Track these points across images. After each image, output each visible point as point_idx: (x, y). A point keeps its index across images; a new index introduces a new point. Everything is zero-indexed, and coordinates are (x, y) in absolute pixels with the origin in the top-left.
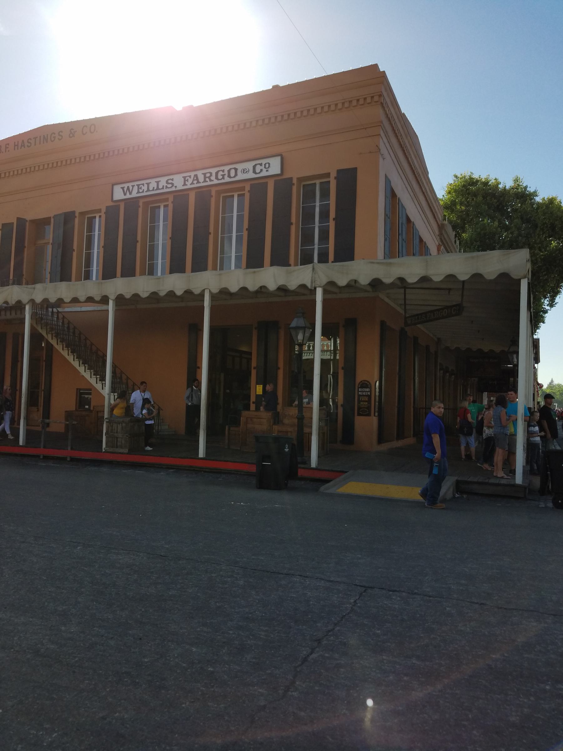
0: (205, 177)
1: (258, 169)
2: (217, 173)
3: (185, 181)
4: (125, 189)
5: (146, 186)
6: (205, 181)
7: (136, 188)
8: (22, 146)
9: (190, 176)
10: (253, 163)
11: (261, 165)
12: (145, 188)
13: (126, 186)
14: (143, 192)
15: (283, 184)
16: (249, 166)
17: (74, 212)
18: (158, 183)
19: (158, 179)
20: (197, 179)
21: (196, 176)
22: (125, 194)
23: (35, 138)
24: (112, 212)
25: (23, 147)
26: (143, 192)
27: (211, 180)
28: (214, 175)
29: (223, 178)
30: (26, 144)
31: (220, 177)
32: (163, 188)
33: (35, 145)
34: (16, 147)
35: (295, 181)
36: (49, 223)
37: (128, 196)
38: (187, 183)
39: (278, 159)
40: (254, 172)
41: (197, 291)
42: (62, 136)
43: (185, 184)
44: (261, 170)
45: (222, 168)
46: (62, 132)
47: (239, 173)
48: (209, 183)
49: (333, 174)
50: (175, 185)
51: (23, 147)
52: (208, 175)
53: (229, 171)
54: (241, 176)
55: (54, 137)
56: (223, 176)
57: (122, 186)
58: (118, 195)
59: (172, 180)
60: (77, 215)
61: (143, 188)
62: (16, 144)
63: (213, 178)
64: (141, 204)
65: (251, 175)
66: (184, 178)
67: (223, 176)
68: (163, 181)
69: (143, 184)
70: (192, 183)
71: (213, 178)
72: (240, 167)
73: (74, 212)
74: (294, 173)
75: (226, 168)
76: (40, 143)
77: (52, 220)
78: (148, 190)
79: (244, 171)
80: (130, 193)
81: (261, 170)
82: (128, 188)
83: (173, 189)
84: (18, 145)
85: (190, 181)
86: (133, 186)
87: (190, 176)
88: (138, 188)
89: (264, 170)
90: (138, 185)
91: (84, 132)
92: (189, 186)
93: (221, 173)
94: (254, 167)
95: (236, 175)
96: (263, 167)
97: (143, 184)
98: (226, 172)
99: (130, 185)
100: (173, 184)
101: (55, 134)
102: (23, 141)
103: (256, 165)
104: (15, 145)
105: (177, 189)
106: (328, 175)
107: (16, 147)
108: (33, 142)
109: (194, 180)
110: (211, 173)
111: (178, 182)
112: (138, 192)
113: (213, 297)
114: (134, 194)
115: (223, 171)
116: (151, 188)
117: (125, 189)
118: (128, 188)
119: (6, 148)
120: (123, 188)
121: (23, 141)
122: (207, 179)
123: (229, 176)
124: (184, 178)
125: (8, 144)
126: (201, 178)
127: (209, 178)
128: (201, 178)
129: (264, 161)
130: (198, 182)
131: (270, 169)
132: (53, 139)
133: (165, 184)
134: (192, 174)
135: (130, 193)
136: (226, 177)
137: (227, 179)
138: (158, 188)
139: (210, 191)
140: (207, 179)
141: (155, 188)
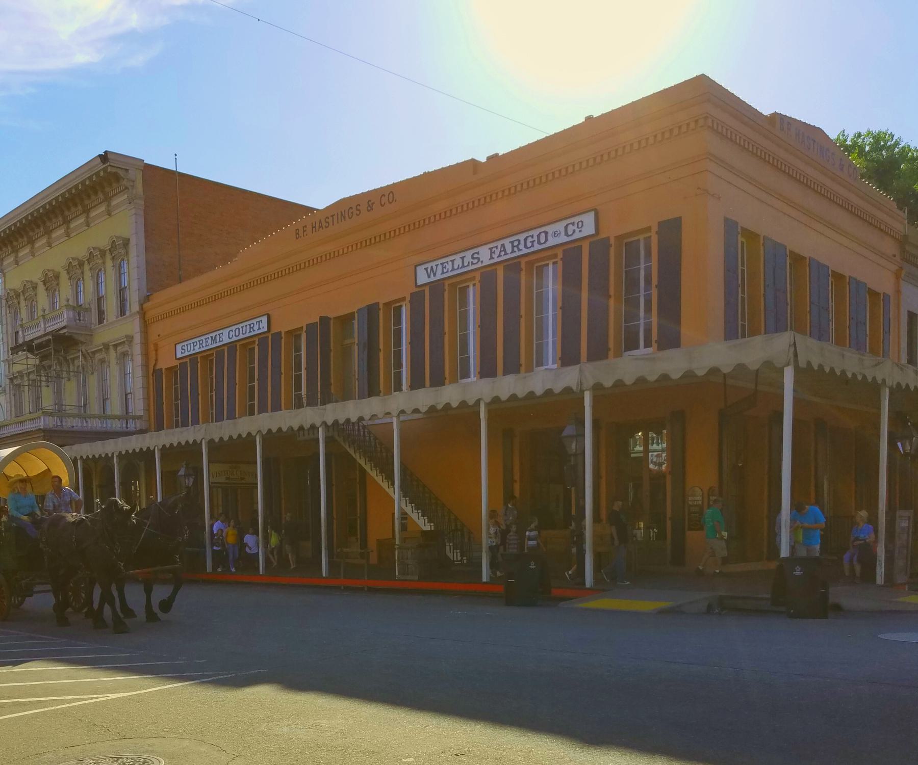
0: (513, 247)
1: (571, 229)
2: (525, 240)
3: (491, 253)
4: (429, 270)
5: (450, 263)
6: (513, 251)
7: (440, 267)
9: (496, 247)
10: (564, 223)
11: (573, 224)
12: (449, 267)
13: (429, 265)
15: (599, 245)
16: (560, 226)
17: (378, 303)
18: (463, 258)
20: (505, 250)
21: (503, 245)
22: (429, 277)
24: (416, 299)
27: (519, 250)
28: (522, 242)
29: (533, 246)
31: (529, 244)
35: (612, 241)
36: (354, 319)
37: (433, 279)
39: (592, 214)
40: (567, 234)
43: (492, 258)
44: (574, 231)
45: (530, 233)
47: (550, 237)
48: (518, 254)
49: (655, 229)
52: (516, 243)
53: (539, 236)
54: (552, 242)
56: (532, 242)
59: (478, 253)
60: (381, 306)
63: (521, 246)
64: (446, 287)
65: (563, 239)
66: (491, 249)
67: (532, 242)
70: (500, 256)
71: (521, 246)
72: (550, 229)
73: (378, 303)
74: (611, 231)
75: (535, 233)
77: (356, 315)
78: (453, 269)
79: (555, 234)
80: (435, 275)
81: (574, 231)
83: (480, 265)
85: (497, 252)
86: (437, 265)
87: (496, 247)
89: (577, 230)
90: (442, 264)
92: (496, 260)
93: (530, 239)
94: (566, 227)
96: (575, 227)
98: (536, 238)
99: (433, 264)
100: (478, 259)
103: (567, 225)
106: (649, 229)
110: (519, 241)
112: (443, 273)
114: (439, 276)
115: (532, 236)
116: (456, 267)
117: (429, 270)
120: (426, 269)
122: (516, 249)
123: (539, 243)
124: (491, 249)
126: (509, 248)
127: (517, 246)
128: (509, 248)
129: (576, 220)
130: (506, 254)
131: (583, 229)
134: (499, 244)
135: (435, 275)
136: (535, 243)
137: (537, 247)
139: (520, 262)
140: (516, 249)
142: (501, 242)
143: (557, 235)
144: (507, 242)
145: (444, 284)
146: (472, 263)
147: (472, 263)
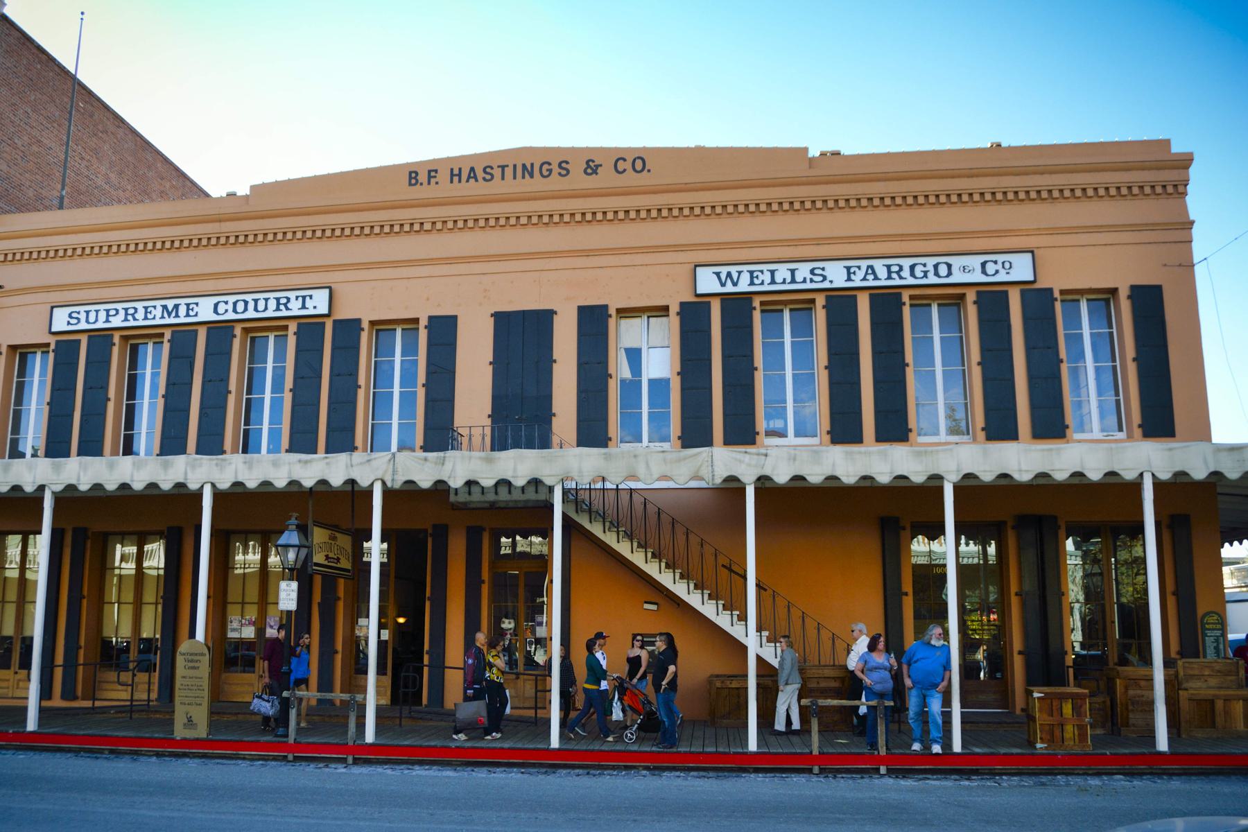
0: (889, 272)
1: (991, 268)
3: (849, 273)
4: (723, 277)
6: (889, 278)
8: (469, 177)
12: (767, 277)
13: (724, 271)
14: (762, 283)
16: (976, 261)
19: (793, 266)
20: (874, 273)
22: (723, 285)
23: (503, 167)
25: (472, 181)
26: (762, 283)
30: (480, 174)
32: (804, 281)
33: (503, 178)
34: (456, 179)
37: (729, 288)
38: (853, 277)
40: (984, 272)
41: (1129, 475)
42: (568, 172)
43: (849, 279)
44: (997, 272)
45: (922, 260)
46: (567, 163)
48: (898, 282)
50: (829, 278)
51: (472, 181)
54: (957, 277)
55: (550, 171)
57: (717, 269)
58: (708, 282)
59: (823, 269)
61: (154, 312)
62: (456, 172)
65: (978, 277)
66: (848, 268)
68: (803, 270)
69: (762, 272)
70: (864, 279)
72: (957, 262)
75: (931, 262)
76: (515, 178)
78: (773, 282)
81: (997, 272)
82: (729, 275)
83: (826, 285)
84: (459, 175)
85: (860, 274)
87: (859, 268)
88: (188, 309)
89: (1003, 272)
91: (620, 169)
92: (857, 283)
95: (950, 274)
96: (999, 266)
97: (762, 272)
98: (930, 268)
99: (734, 270)
100: (825, 278)
101: (549, 164)
102: (472, 169)
104: (452, 175)
105: (834, 285)
107: (456, 179)
108: (497, 172)
109: (867, 273)
111: (836, 276)
113: (1158, 485)
114: (744, 286)
117: (723, 277)
118: (729, 275)
119: (430, 177)
120: (718, 274)
121: (472, 169)
122: (894, 275)
123: (937, 274)
125: (436, 171)
128: (882, 273)
129: (1000, 258)
130: (876, 278)
132: (546, 173)
133: (809, 276)
134: (864, 264)
135: (735, 284)
136: (931, 274)
137: (932, 279)
138: (793, 281)
139: (900, 294)
141: (789, 280)
142: (870, 262)
143: (968, 270)
144: (879, 266)
145: (750, 300)
146: (812, 281)
147: (812, 281)
